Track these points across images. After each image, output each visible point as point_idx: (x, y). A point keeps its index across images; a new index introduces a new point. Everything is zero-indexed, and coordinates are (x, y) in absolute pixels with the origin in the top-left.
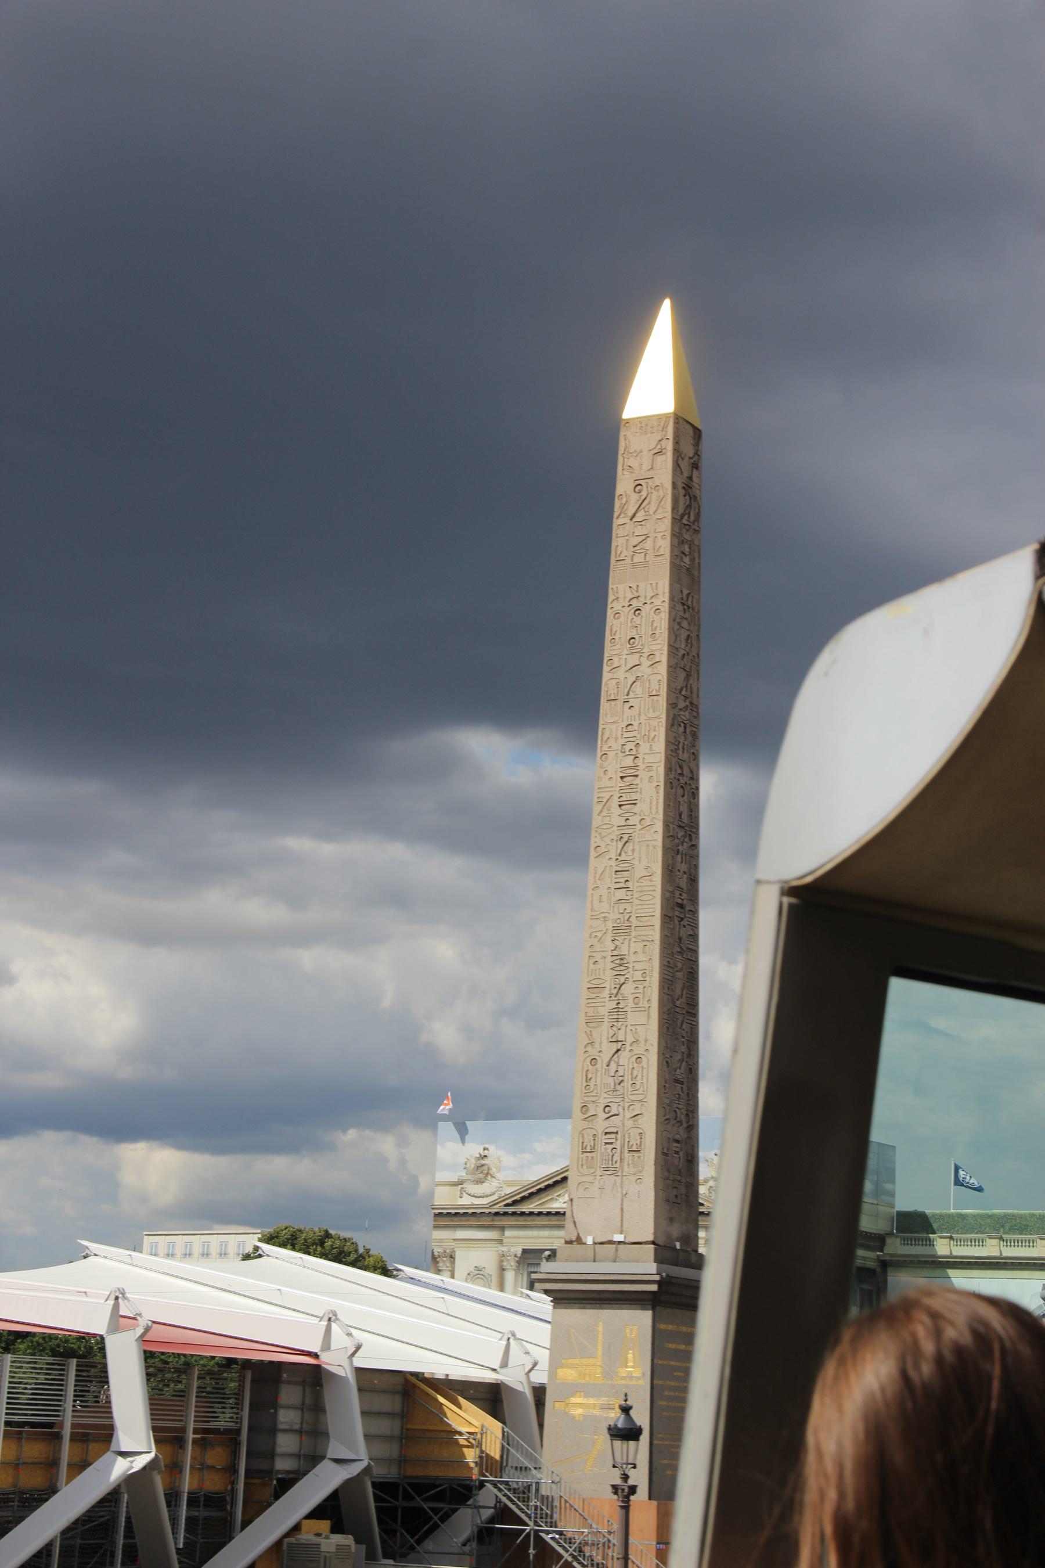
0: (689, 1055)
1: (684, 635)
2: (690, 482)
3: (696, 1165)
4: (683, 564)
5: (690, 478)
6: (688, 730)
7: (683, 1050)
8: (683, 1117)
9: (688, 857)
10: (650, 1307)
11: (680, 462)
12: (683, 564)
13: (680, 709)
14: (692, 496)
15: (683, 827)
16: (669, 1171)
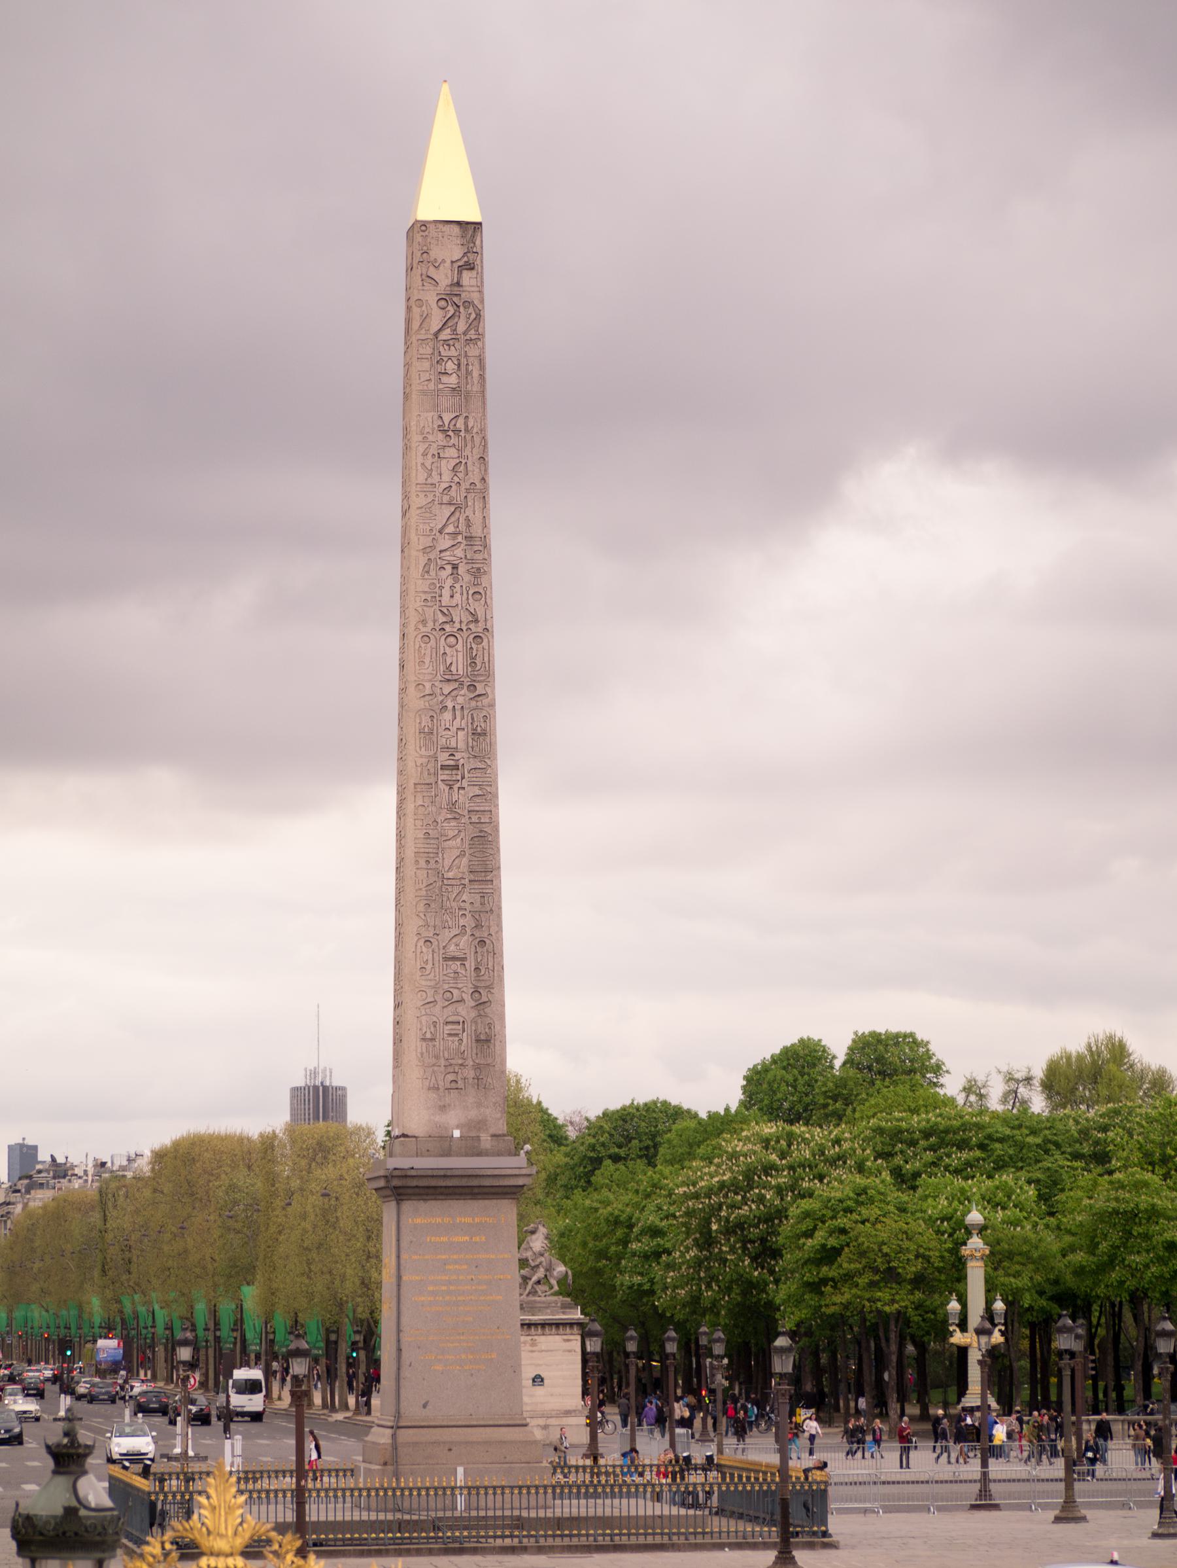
0: (478, 926)
1: (446, 467)
2: (456, 289)
3: (497, 1043)
4: (441, 386)
5: (458, 284)
6: (462, 569)
7: (461, 924)
9: (466, 712)
10: (394, 1203)
11: (432, 272)
12: (441, 386)
13: (441, 552)
14: (461, 304)
15: (455, 680)
16: (437, 1057)
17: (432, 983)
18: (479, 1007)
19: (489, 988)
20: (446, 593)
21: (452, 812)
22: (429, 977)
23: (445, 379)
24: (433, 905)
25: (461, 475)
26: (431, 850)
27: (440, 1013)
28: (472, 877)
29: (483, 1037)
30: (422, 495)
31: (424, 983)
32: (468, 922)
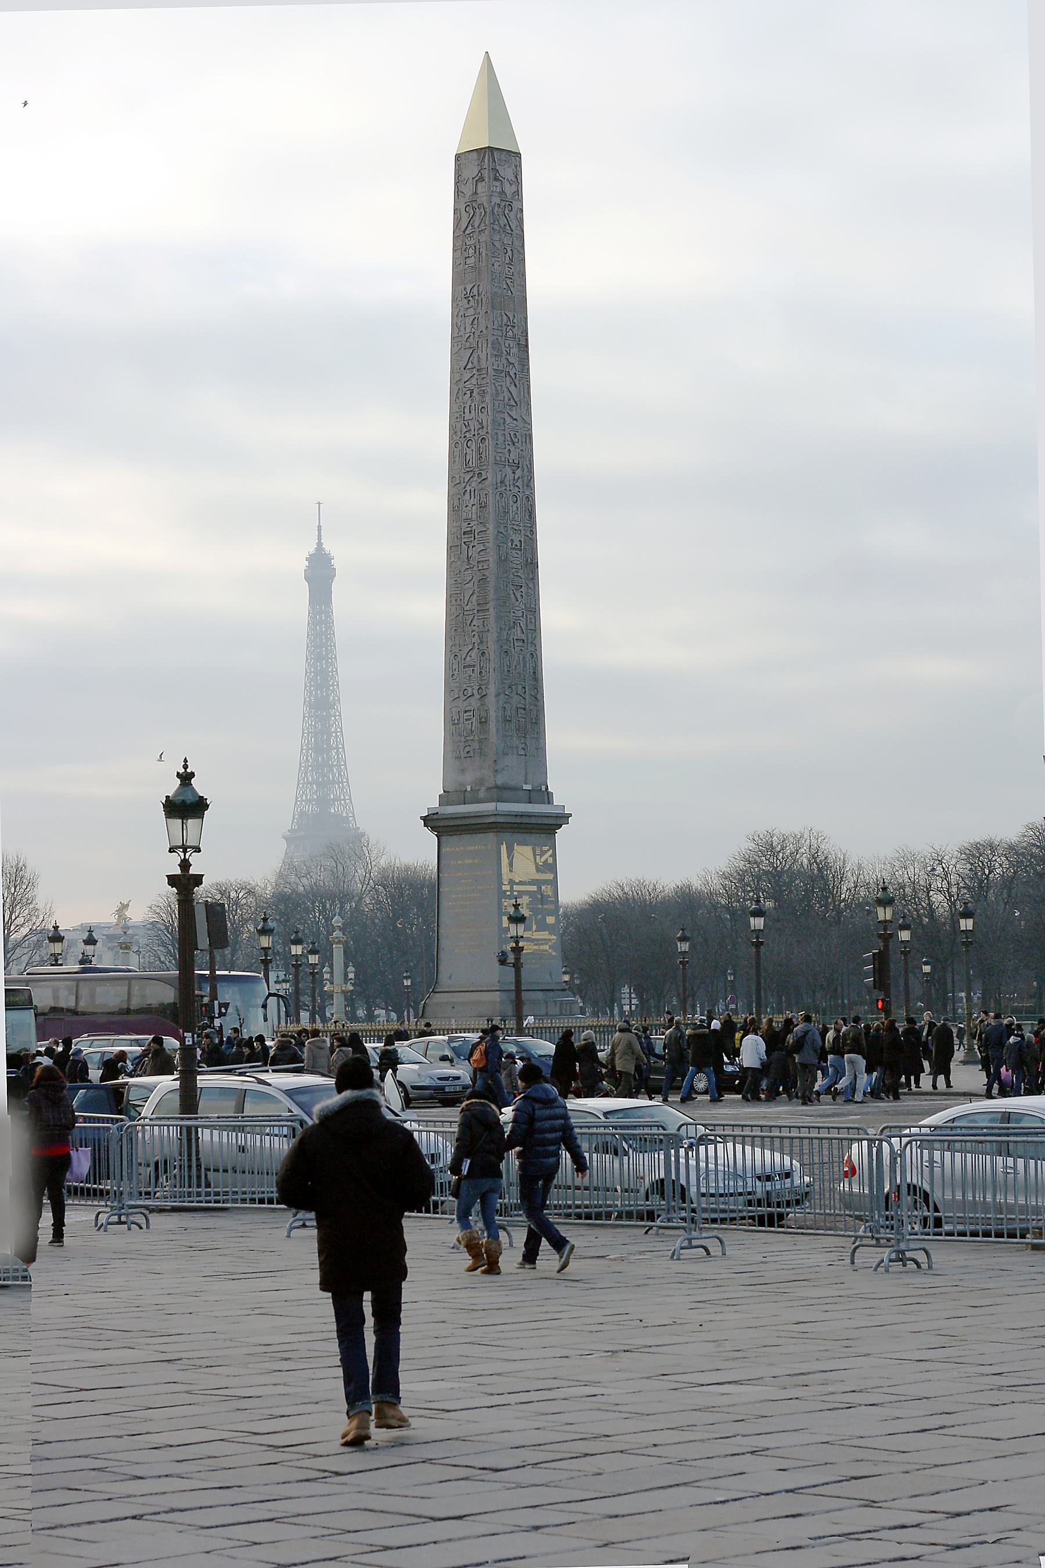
0: (482, 642)
1: (469, 321)
6: (475, 394)
8: (475, 692)
11: (463, 188)
12: (466, 266)
16: (461, 735)
17: (457, 685)
18: (483, 698)
19: (487, 684)
20: (467, 410)
21: (469, 564)
22: (457, 680)
23: (468, 261)
24: (459, 630)
25: (475, 326)
26: (458, 592)
27: (462, 705)
28: (479, 608)
29: (483, 720)
30: (455, 344)
31: (453, 685)
32: (476, 640)
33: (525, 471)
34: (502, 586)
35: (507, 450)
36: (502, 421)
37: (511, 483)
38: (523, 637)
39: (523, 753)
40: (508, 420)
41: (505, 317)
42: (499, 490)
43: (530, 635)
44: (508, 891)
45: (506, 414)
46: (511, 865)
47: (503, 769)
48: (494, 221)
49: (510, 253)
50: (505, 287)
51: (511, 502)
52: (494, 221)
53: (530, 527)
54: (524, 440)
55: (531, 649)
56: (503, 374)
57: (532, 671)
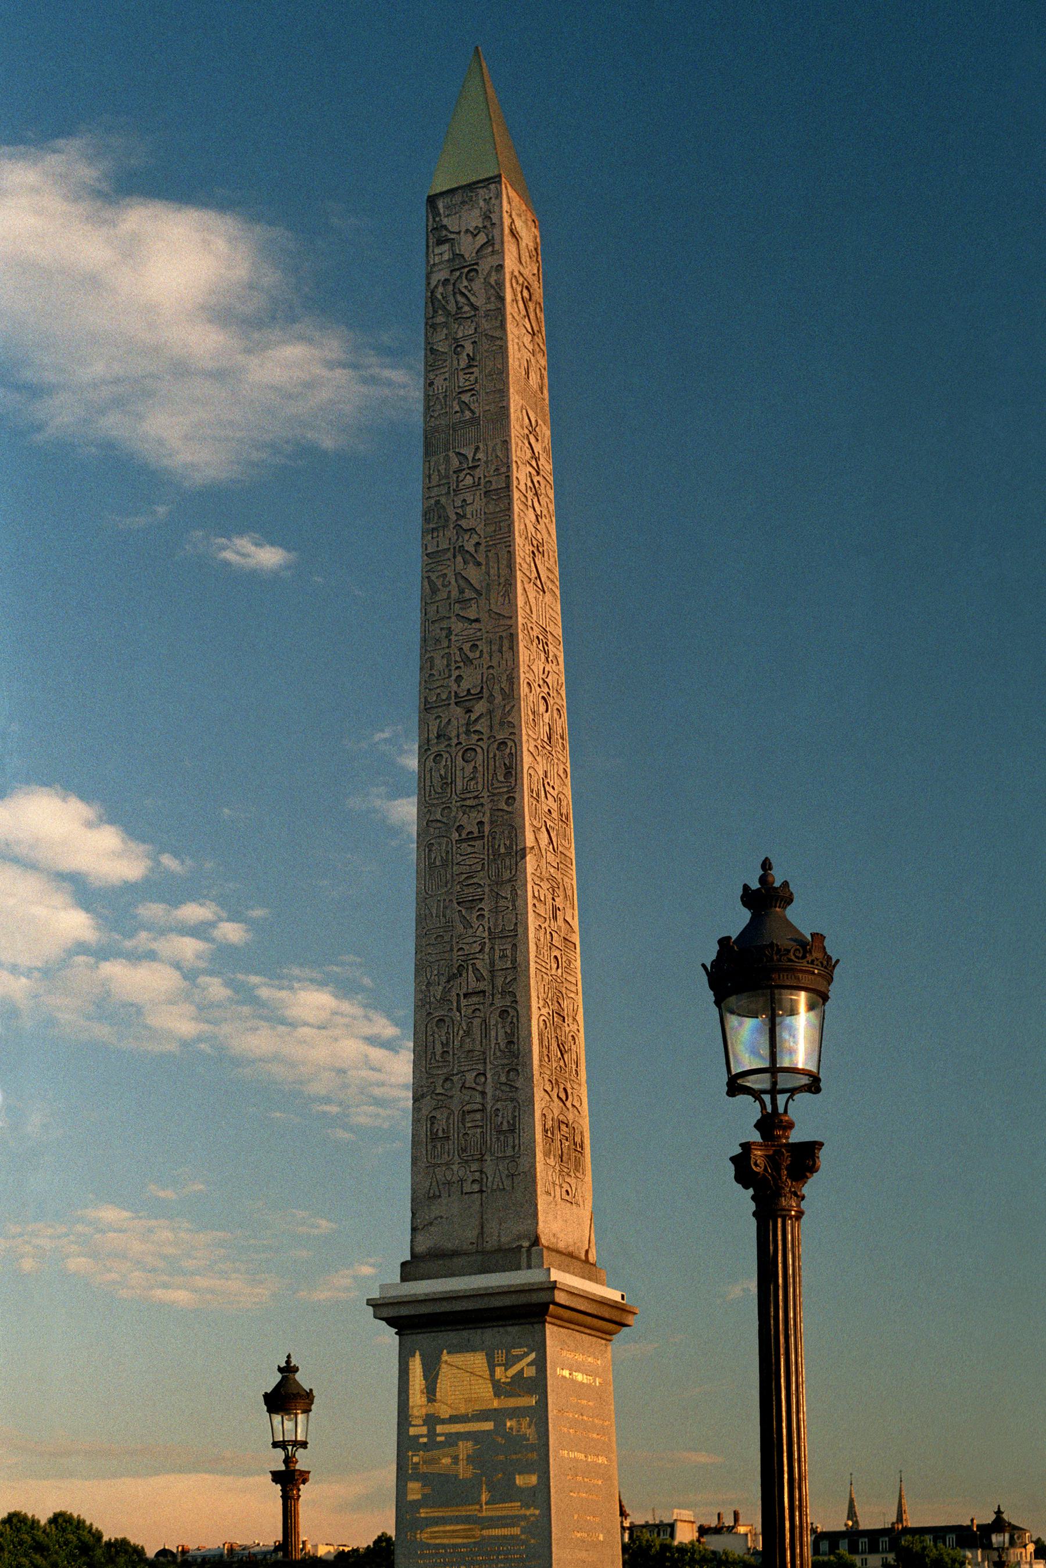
33: (498, 698)
34: (434, 911)
35: (453, 678)
36: (444, 633)
37: (463, 729)
38: (482, 986)
39: (476, 1187)
40: (457, 626)
41: (455, 462)
42: (434, 749)
43: (499, 981)
44: (422, 1436)
45: (454, 619)
46: (430, 1391)
47: (431, 1224)
48: (435, 312)
49: (469, 348)
50: (457, 408)
51: (460, 761)
52: (435, 312)
53: (508, 792)
54: (495, 648)
55: (499, 1002)
56: (449, 555)
57: (503, 1046)
